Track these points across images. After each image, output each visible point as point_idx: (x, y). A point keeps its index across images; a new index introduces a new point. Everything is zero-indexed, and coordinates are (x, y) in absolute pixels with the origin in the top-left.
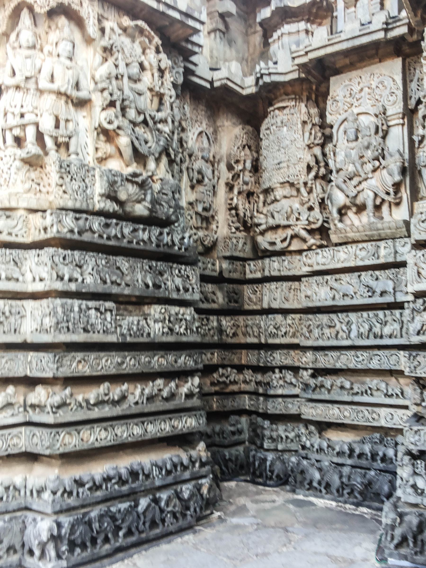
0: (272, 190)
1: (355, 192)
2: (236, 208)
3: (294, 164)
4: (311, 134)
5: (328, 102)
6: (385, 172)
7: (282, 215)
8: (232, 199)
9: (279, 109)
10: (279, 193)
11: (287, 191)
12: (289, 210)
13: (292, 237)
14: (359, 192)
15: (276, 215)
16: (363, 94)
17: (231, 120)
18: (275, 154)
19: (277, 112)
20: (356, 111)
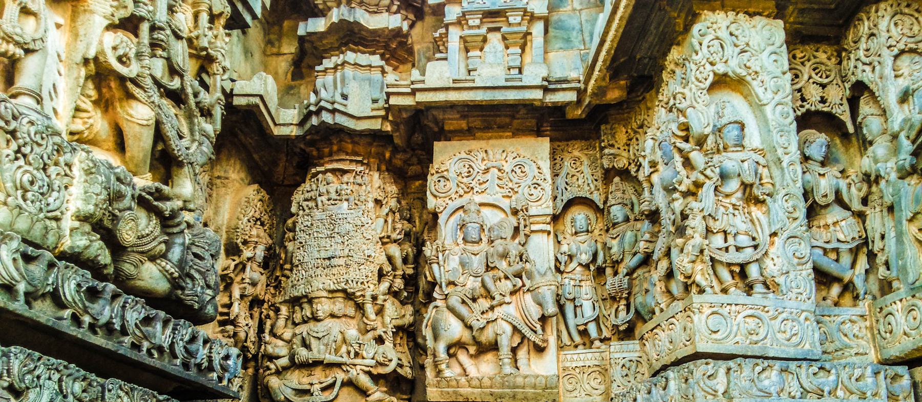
0: (310, 301)
1: (482, 323)
2: (233, 323)
3: (360, 264)
4: (386, 221)
5: (429, 177)
6: (528, 296)
7: (327, 345)
8: (229, 306)
9: (333, 171)
10: (323, 307)
11: (340, 306)
12: (340, 337)
13: (344, 384)
14: (488, 322)
15: (314, 343)
16: (488, 176)
17: (238, 172)
18: (323, 243)
19: (330, 176)
20: (478, 199)
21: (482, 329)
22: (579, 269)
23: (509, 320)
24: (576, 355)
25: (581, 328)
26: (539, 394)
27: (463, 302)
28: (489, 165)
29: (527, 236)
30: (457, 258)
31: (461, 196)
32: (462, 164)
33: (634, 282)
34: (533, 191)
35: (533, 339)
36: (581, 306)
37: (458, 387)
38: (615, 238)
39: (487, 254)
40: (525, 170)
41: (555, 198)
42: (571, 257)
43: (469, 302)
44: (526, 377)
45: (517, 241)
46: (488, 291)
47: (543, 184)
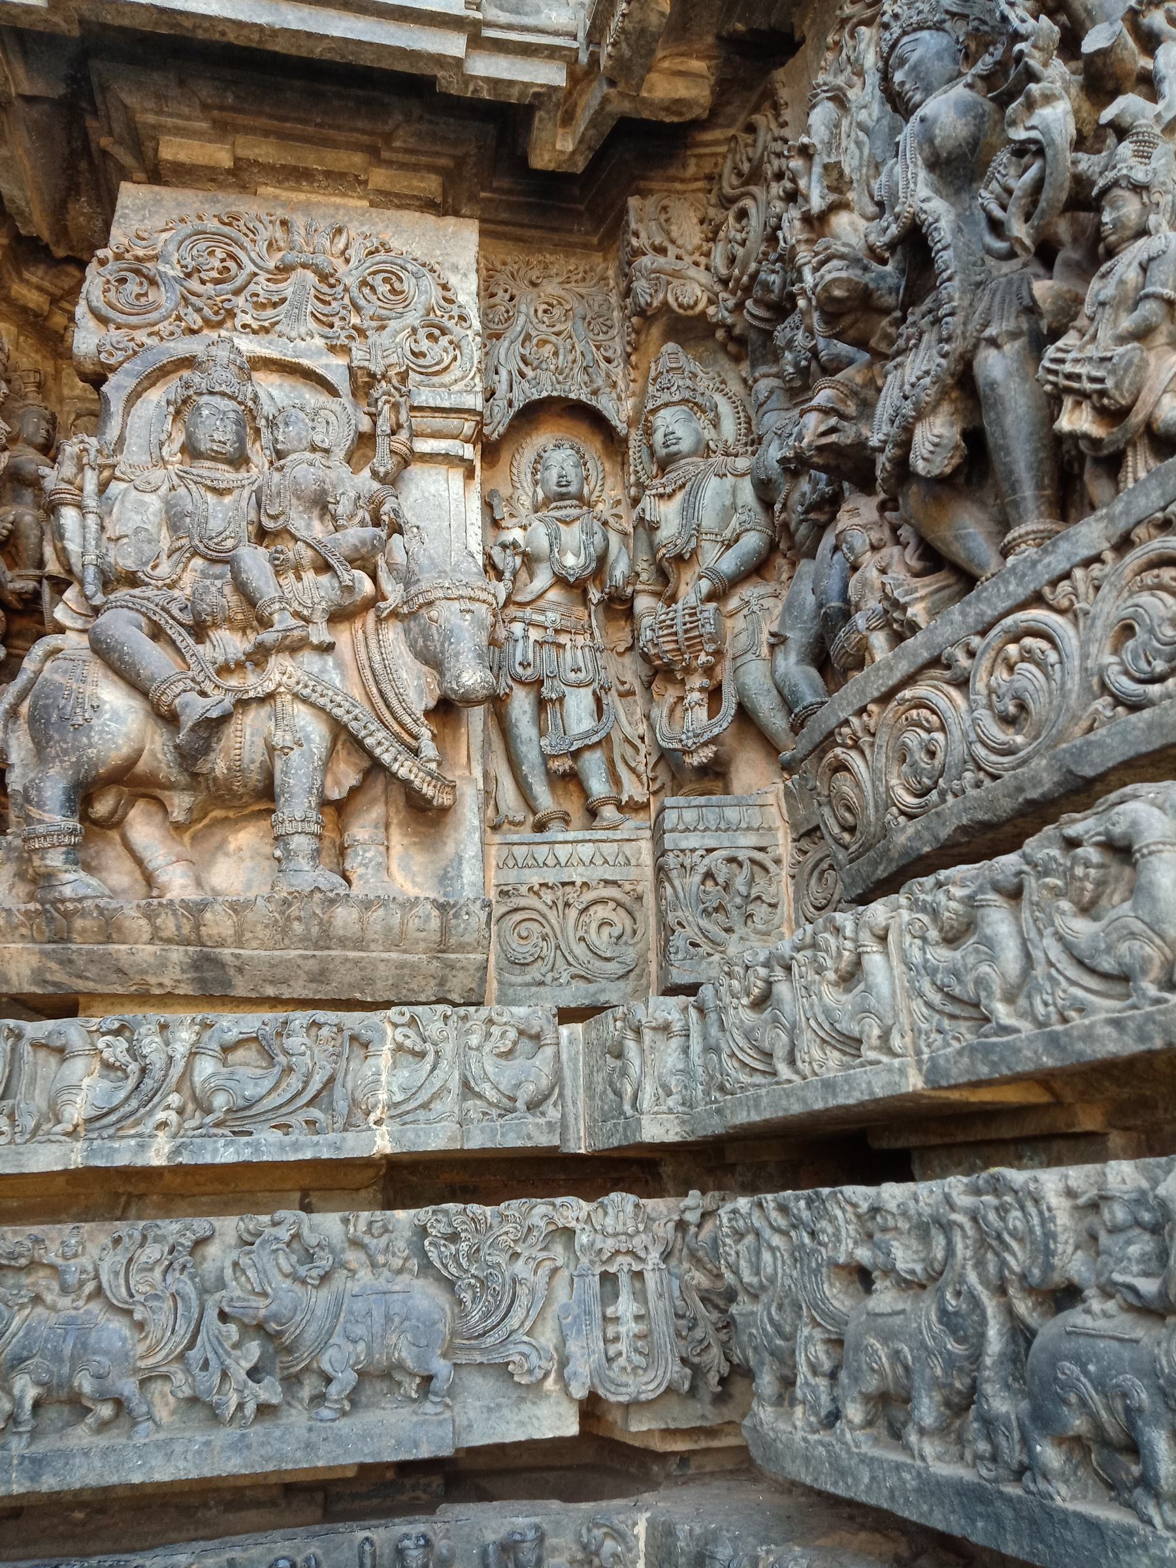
14: (243, 704)
16: (288, 288)
20: (249, 345)
21: (213, 726)
23: (322, 701)
24: (546, 848)
25: (557, 765)
26: (414, 968)
27: (157, 633)
28: (292, 257)
29: (405, 463)
30: (154, 502)
31: (193, 332)
32: (203, 245)
33: (729, 623)
34: (424, 345)
35: (403, 772)
36: (561, 700)
37: (109, 940)
38: (670, 496)
39: (258, 492)
40: (406, 288)
41: (490, 395)
42: (530, 560)
44: (367, 905)
45: (366, 473)
46: (248, 598)
47: (458, 331)
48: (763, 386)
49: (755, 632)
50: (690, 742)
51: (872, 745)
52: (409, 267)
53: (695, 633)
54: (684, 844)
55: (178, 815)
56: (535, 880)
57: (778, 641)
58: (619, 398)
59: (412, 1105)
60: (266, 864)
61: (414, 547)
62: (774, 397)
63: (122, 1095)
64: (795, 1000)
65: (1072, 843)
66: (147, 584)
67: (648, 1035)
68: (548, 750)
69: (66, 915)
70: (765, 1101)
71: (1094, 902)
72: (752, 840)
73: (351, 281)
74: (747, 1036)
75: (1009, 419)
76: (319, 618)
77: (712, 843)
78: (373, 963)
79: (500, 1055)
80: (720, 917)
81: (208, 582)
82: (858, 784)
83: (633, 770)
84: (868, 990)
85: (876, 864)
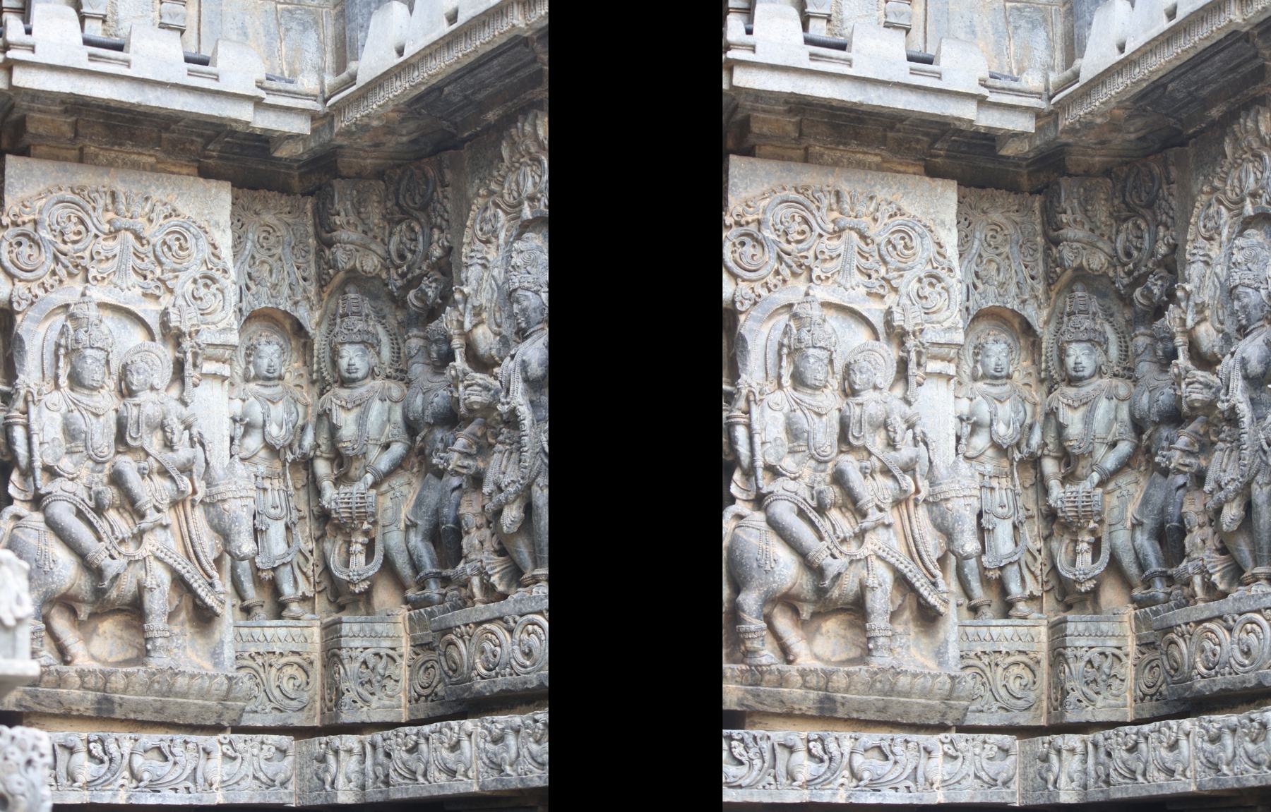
20: (821, 293)
22: (990, 453)
23: (893, 560)
24: (985, 629)
26: (931, 707)
37: (780, 685)
43: (813, 515)
48: (1142, 341)
49: (1123, 510)
50: (1081, 577)
51: (1190, 639)
52: (916, 228)
53: (1089, 509)
54: (1077, 644)
55: (805, 615)
56: (979, 650)
57: (1137, 525)
58: (1039, 307)
59: (952, 781)
60: (842, 641)
61: (936, 461)
62: (1147, 352)
63: (823, 770)
64: (1148, 751)
65: (1252, 720)
66: (783, 475)
67: (1065, 754)
68: (986, 565)
69: (762, 673)
70: (1130, 790)
71: (1256, 739)
72: (1113, 642)
73: (882, 239)
74: (1124, 763)
75: (1262, 521)
76: (887, 507)
77: (1092, 643)
78: (912, 704)
79: (989, 759)
80: (1093, 686)
81: (818, 474)
82: (1181, 654)
83: (1032, 573)
84: (1180, 753)
85: (1186, 690)
